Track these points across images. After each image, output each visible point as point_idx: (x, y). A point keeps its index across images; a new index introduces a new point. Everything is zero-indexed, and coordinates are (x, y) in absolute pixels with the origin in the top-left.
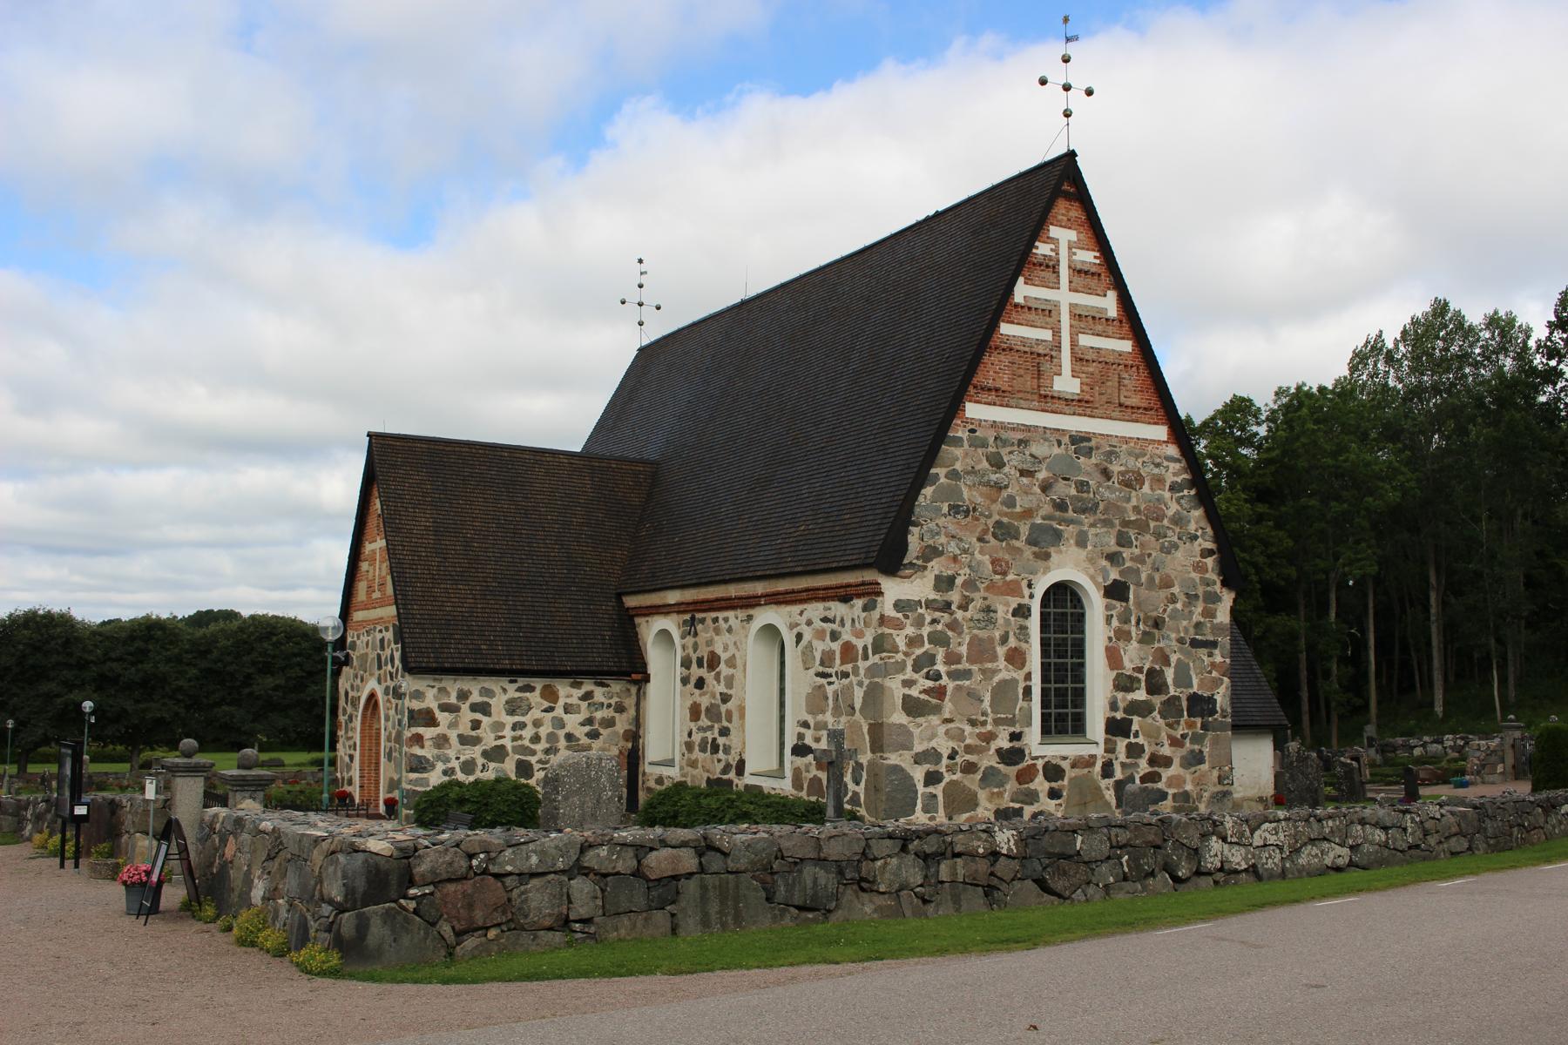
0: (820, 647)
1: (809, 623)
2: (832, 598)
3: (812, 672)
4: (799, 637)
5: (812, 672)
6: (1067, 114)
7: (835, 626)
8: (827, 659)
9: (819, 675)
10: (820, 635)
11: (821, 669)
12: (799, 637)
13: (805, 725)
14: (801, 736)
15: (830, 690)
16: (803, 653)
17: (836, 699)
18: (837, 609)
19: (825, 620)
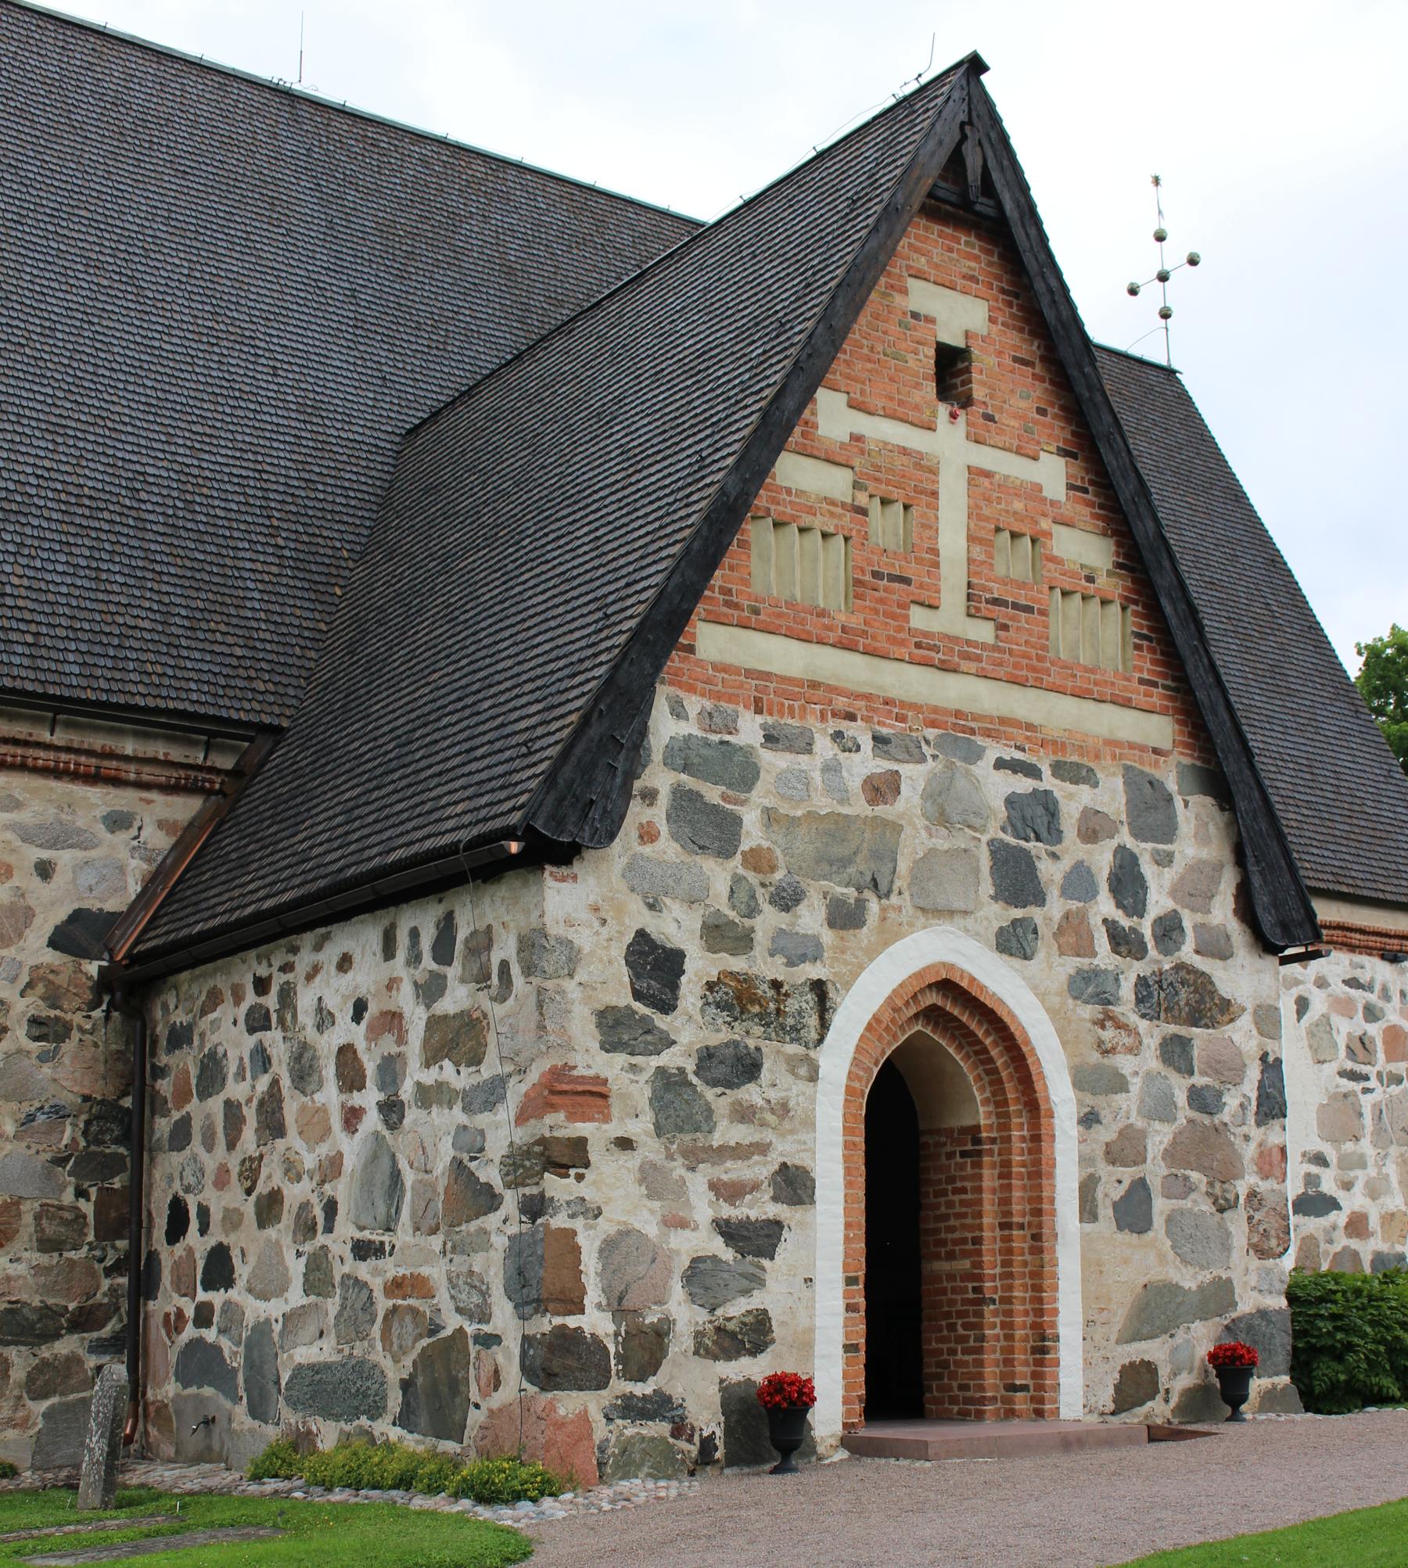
0: (1345, 1028)
1: (1321, 983)
2: (1368, 950)
3: (1331, 1069)
4: (1302, 1005)
5: (1331, 1069)
6: (1165, 315)
7: (1373, 997)
8: (1361, 1046)
9: (1343, 1074)
10: (1345, 1007)
11: (1349, 1065)
12: (1302, 1005)
13: (1320, 1160)
14: (1311, 1180)
15: (1367, 1101)
16: (1311, 1034)
17: (1379, 1115)
18: (1376, 969)
19: (1353, 983)
